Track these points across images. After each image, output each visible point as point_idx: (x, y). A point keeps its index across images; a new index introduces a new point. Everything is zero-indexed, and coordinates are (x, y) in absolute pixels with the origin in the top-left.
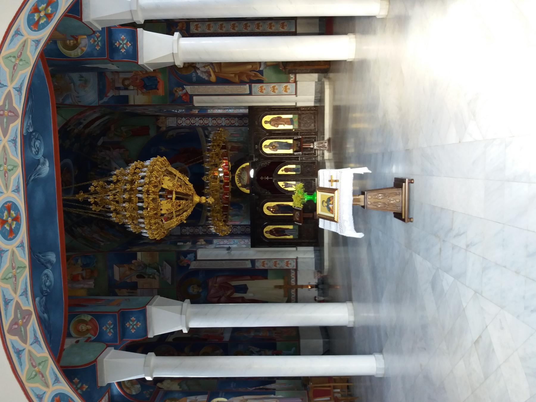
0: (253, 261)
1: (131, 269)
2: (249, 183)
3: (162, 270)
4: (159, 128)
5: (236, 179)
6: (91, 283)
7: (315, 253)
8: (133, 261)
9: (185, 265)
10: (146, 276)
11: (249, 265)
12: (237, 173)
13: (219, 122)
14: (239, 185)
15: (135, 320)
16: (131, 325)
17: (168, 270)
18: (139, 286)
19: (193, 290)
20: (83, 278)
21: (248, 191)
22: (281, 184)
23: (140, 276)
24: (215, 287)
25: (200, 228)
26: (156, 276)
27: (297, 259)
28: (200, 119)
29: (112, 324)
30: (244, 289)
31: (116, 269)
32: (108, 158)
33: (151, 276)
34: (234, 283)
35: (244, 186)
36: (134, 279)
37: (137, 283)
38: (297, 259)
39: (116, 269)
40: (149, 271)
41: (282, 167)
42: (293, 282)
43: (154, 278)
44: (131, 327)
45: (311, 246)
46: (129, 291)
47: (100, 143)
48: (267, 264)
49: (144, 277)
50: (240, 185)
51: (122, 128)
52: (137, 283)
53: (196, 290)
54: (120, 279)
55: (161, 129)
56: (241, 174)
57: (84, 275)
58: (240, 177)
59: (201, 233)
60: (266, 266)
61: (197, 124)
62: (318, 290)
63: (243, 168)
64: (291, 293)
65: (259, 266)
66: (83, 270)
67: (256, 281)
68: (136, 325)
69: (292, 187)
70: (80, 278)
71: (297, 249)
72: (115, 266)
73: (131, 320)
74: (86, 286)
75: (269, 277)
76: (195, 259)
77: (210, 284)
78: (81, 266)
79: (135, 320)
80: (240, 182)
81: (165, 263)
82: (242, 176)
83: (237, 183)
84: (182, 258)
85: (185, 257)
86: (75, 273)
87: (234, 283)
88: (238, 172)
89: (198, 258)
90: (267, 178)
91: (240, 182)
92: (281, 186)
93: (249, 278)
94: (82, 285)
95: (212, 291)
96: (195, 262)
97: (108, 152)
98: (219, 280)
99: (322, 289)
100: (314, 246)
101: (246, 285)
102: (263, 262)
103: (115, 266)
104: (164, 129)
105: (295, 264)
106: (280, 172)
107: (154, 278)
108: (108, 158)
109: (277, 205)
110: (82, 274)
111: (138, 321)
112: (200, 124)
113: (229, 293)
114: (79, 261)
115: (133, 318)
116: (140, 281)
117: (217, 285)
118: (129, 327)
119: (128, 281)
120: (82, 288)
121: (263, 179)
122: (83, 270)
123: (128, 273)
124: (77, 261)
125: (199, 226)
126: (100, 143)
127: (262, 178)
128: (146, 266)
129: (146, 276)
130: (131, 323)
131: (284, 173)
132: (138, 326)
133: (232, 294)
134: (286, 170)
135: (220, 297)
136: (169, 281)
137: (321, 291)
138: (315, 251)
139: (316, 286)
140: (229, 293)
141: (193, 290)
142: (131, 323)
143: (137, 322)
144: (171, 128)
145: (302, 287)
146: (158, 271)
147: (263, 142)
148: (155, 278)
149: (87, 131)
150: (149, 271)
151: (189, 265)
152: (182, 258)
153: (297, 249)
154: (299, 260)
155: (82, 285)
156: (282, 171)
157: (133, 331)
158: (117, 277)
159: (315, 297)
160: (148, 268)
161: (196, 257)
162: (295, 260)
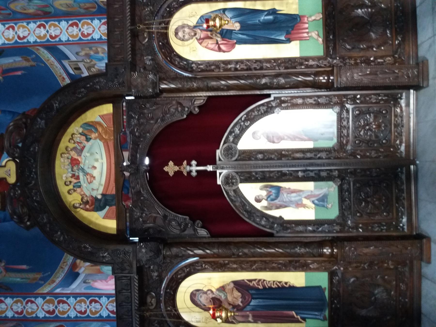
2: (112, 191)
13: (86, 30)
21: (111, 225)
25: (40, 301)
28: (39, 27)
35: (97, 205)
41: (251, 119)
59: (41, 315)
61: (32, 39)
69: (299, 205)
82: (86, 160)
90: (194, 168)
92: (252, 201)
109: (239, 285)
112: (39, 37)
121: (178, 174)
125: (37, 296)
127: (171, 168)
147: (171, 14)
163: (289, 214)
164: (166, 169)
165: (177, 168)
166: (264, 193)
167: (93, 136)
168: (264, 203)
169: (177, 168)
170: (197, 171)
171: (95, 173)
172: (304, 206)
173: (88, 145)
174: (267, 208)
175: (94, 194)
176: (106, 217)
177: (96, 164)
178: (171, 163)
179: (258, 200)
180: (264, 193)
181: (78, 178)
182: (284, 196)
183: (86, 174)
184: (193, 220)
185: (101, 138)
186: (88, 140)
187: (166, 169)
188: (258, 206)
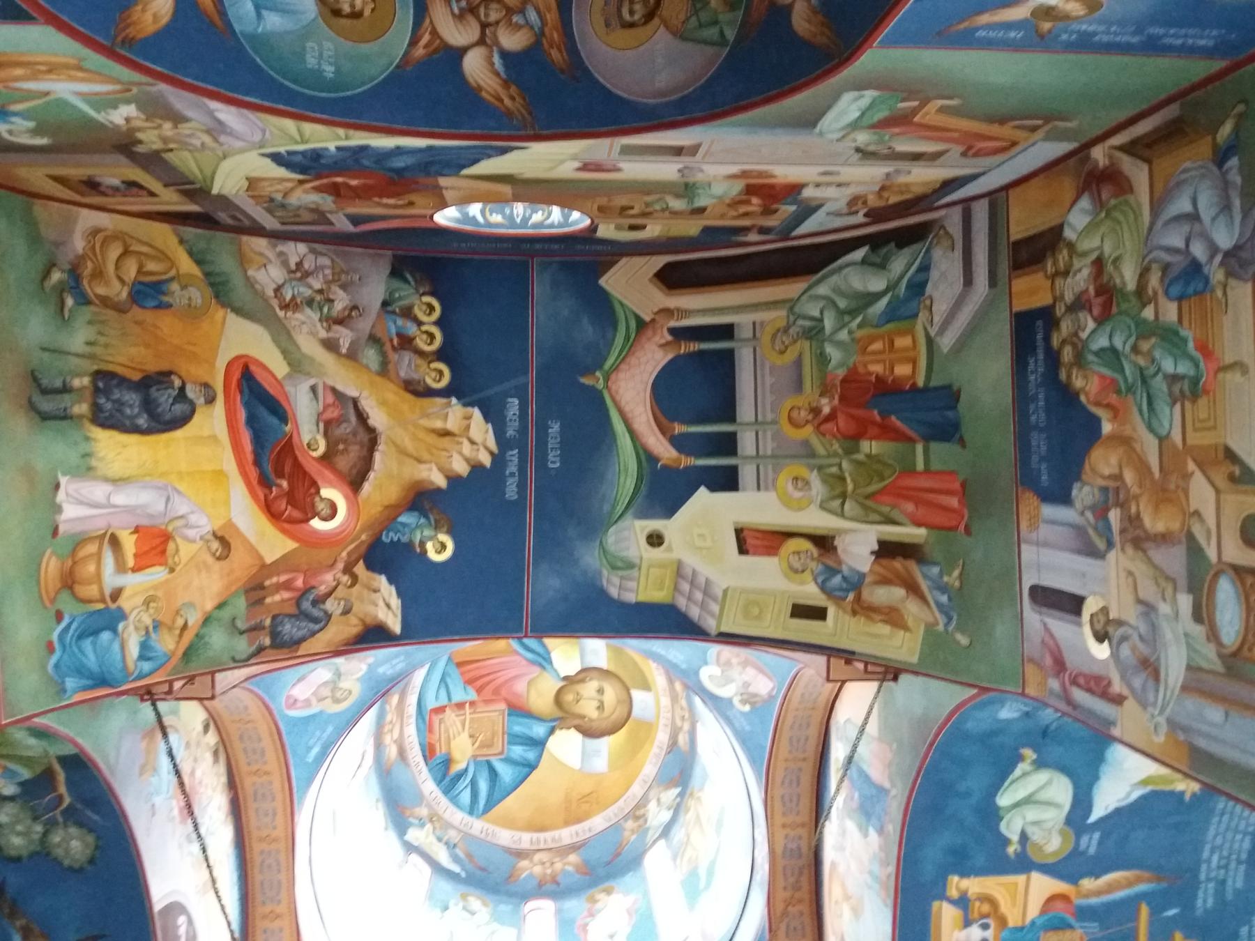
20: (115, 542)
66: (116, 594)
70: (129, 543)
74: (98, 491)
78: (122, 615)
86: (156, 574)
110: (121, 568)
114: (134, 650)
120: (118, 481)
122: (116, 594)
124: (146, 651)
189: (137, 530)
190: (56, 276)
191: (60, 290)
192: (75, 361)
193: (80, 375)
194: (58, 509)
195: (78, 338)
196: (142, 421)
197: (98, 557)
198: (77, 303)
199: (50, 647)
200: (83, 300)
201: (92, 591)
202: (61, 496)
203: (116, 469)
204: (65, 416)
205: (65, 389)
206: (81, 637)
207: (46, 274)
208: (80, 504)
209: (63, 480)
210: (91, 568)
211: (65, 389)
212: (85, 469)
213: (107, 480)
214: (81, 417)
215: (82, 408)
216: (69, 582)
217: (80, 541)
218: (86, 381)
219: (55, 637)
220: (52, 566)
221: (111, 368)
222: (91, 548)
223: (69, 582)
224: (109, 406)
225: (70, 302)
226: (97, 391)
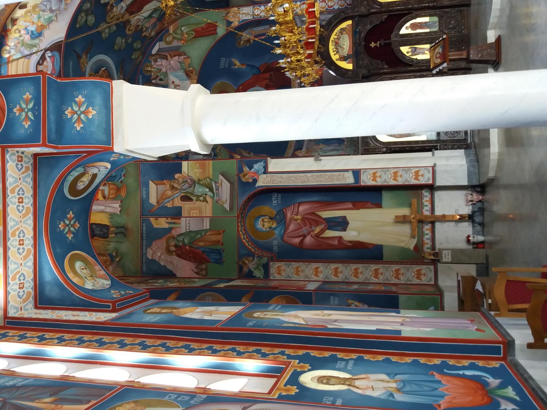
0: (357, 173)
1: (173, 188)
3: (217, 189)
4: (229, 23)
5: (331, 47)
6: (117, 205)
7: (466, 157)
8: (177, 176)
9: (251, 181)
10: (195, 198)
11: (350, 180)
12: (332, 38)
14: (335, 57)
15: (84, 103)
16: (76, 113)
17: (225, 188)
18: (185, 213)
19: (263, 226)
20: (104, 197)
22: (405, 50)
23: (186, 198)
24: (296, 220)
26: (208, 198)
27: (433, 167)
29: (31, 100)
30: (342, 224)
31: (152, 186)
32: (164, 70)
33: (201, 198)
34: (326, 214)
35: (343, 59)
36: (178, 203)
37: (181, 208)
38: (433, 167)
39: (152, 186)
40: (199, 190)
42: (426, 211)
43: (205, 200)
44: (76, 116)
45: (459, 148)
46: (169, 220)
47: (154, 51)
48: (380, 177)
49: (190, 200)
50: (337, 56)
51: (183, 29)
52: (181, 208)
53: (267, 225)
54: (158, 202)
55: (233, 25)
56: (338, 39)
57: (106, 193)
58: (336, 44)
60: (379, 180)
62: (473, 227)
63: (342, 29)
64: (423, 232)
65: (366, 180)
67: (362, 211)
68: (85, 112)
71: (433, 155)
72: (151, 182)
73: (76, 102)
74: (108, 210)
75: (384, 204)
76: (266, 172)
77: (289, 215)
79: (84, 103)
80: (338, 52)
81: (221, 177)
82: (341, 42)
83: (332, 54)
84: (246, 169)
85: (251, 168)
87: (326, 214)
88: (333, 37)
89: (270, 169)
91: (338, 52)
92: (405, 53)
93: (350, 206)
94: (102, 208)
95: (292, 227)
96: (265, 176)
97: (164, 62)
98: (301, 208)
99: (480, 224)
100: (464, 149)
101: (344, 218)
102: (374, 174)
103: (151, 183)
104: (236, 24)
105: (430, 175)
106: (404, 31)
107: (205, 200)
108: (164, 70)
111: (90, 103)
113: (318, 230)
115: (80, 98)
116: (186, 206)
117: (299, 217)
118: (71, 118)
119: (169, 205)
120: (103, 212)
123: (169, 193)
126: (154, 51)
127: (373, 45)
128: (194, 183)
129: (195, 198)
130: (76, 108)
131: (410, 31)
132: (90, 116)
133: (322, 231)
134: (414, 26)
135: (305, 236)
136: (227, 206)
137: (478, 228)
138: (467, 155)
139: (470, 218)
140: (318, 230)
141: (263, 226)
142: (76, 108)
143: (87, 107)
144: (245, 26)
145: (444, 219)
146: (211, 190)
148: (207, 202)
149: (134, 19)
150: (199, 190)
151: (255, 181)
152: (246, 169)
153: (433, 155)
154: (437, 169)
155: (102, 208)
156: (407, 28)
157: (79, 127)
158: (153, 200)
159: (469, 236)
160: (196, 185)
161: (266, 167)
162: (431, 169)
163: (420, 57)
164: (371, 45)
165: (375, 45)
166: (410, 50)
167: (344, 33)
168: (410, 54)
169: (375, 45)
170: (384, 43)
171: (345, 47)
172: (426, 54)
173: (342, 36)
174: (411, 56)
175: (344, 55)
176: (348, 63)
177: (345, 43)
178: (373, 43)
179: (408, 53)
180: (410, 50)
181: (338, 49)
182: (418, 51)
183: (341, 47)
184: (382, 62)
185: (347, 33)
186: (342, 34)
187: (371, 45)
188: (408, 55)
189: (98, 200)
190: (118, 259)
191: (117, 256)
192: (113, 240)
193: (112, 237)
194: (120, 206)
195: (112, 246)
196: (94, 226)
197: (109, 194)
198: (112, 254)
199: (124, 175)
200: (110, 255)
201: (111, 186)
202: (119, 209)
203: (102, 215)
204: (117, 227)
205: (116, 234)
206: (115, 176)
207: (120, 260)
208: (115, 207)
209: (118, 213)
210: (111, 192)
211: (116, 234)
212: (112, 215)
213: (106, 212)
214: (113, 227)
215: (111, 229)
216: (118, 189)
217: (114, 199)
218: (110, 236)
219: (123, 178)
220: (123, 194)
221: (103, 239)
222: (111, 196)
223: (118, 189)
224: (104, 230)
225: (114, 254)
226: (108, 234)
